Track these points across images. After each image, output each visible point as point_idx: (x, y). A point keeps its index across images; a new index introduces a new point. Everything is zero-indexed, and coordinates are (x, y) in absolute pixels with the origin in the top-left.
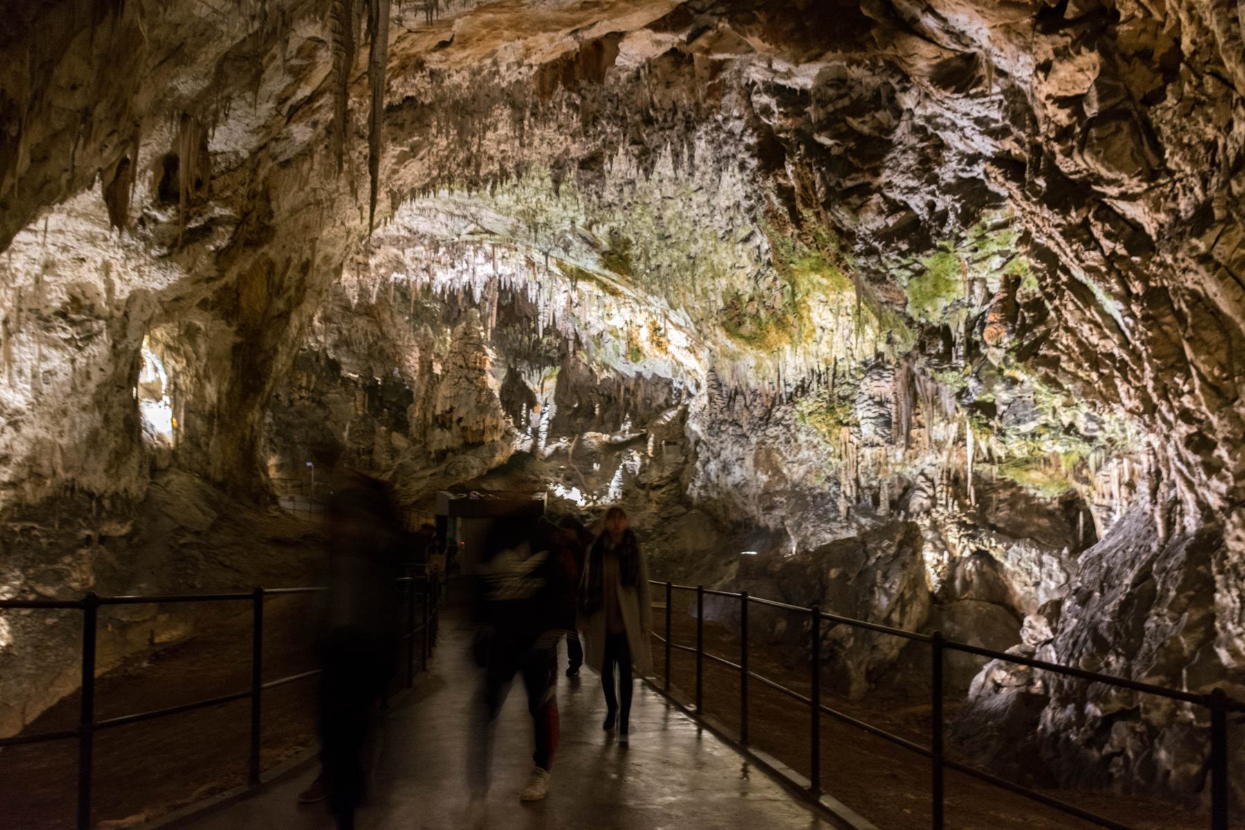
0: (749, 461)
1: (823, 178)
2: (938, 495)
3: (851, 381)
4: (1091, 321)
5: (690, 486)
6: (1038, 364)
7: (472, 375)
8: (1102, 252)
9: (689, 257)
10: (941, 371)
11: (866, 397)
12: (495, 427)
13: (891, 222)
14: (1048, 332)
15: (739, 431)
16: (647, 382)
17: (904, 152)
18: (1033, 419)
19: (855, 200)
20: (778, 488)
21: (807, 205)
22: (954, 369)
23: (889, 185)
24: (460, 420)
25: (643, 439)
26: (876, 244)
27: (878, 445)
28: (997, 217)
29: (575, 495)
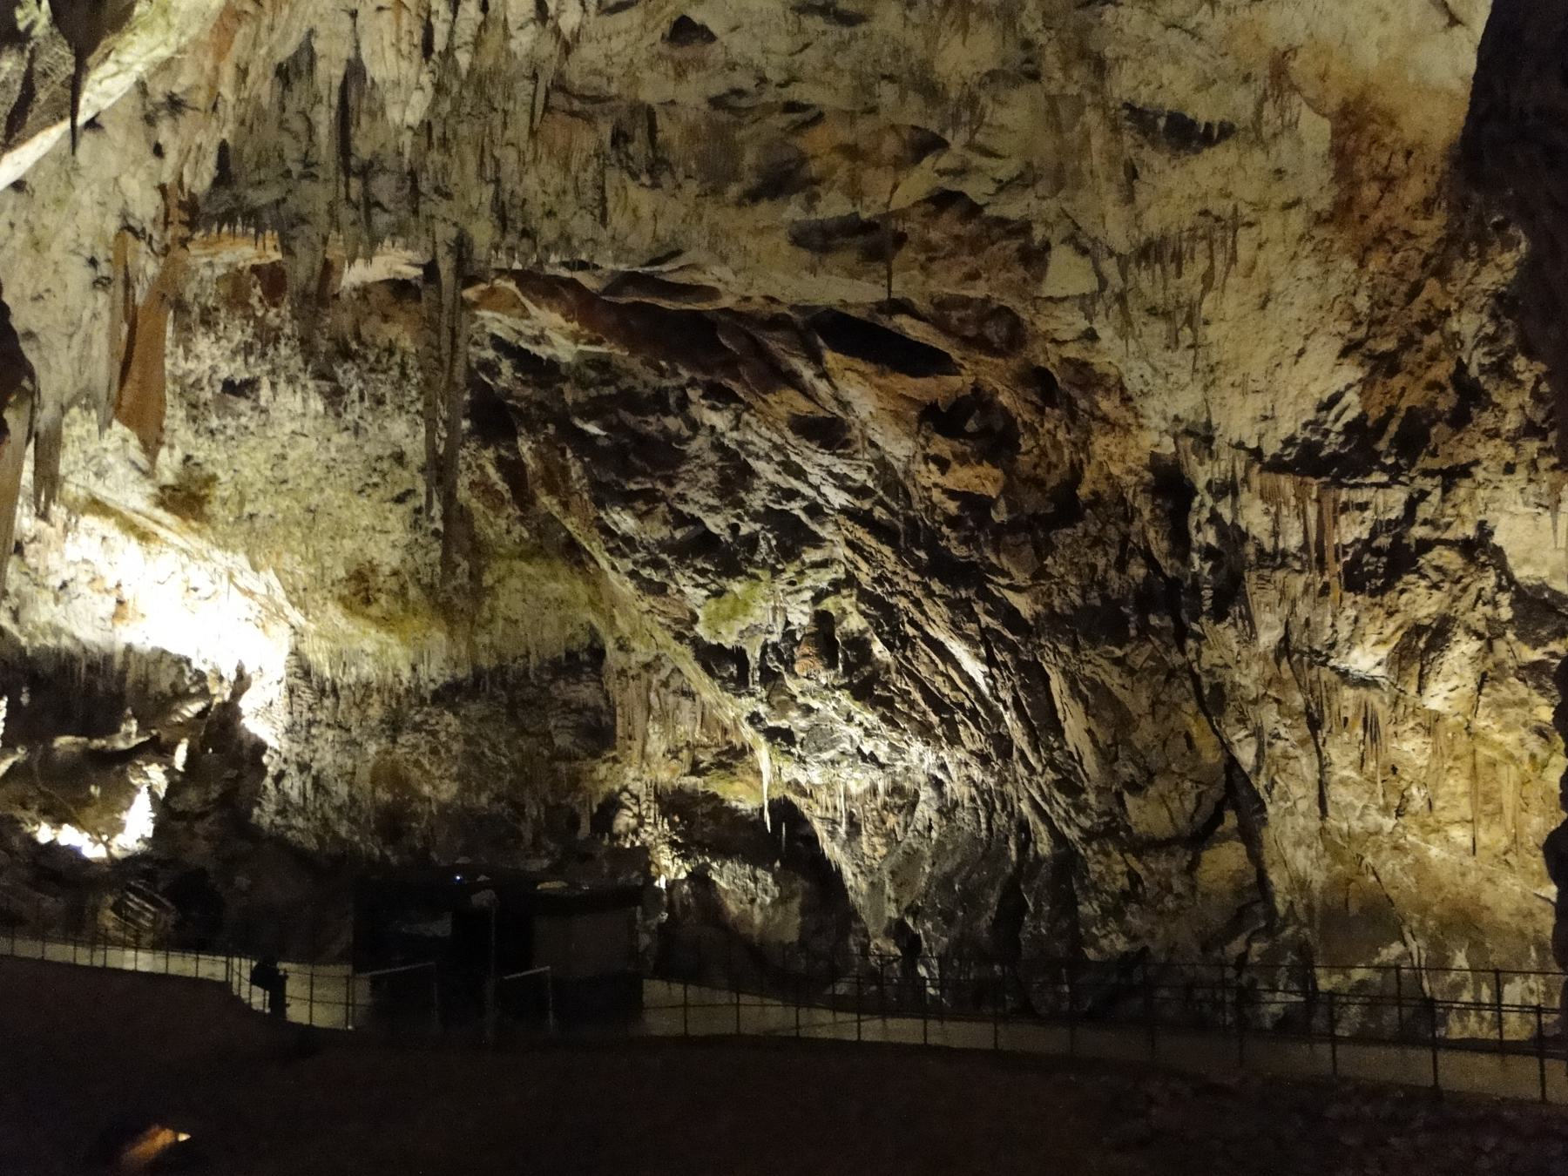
5: (256, 811)
9: (309, 510)
10: (740, 696)
13: (678, 535)
15: (345, 736)
17: (703, 468)
19: (641, 506)
21: (552, 490)
22: (752, 695)
23: (682, 498)
26: (664, 556)
29: (69, 836)
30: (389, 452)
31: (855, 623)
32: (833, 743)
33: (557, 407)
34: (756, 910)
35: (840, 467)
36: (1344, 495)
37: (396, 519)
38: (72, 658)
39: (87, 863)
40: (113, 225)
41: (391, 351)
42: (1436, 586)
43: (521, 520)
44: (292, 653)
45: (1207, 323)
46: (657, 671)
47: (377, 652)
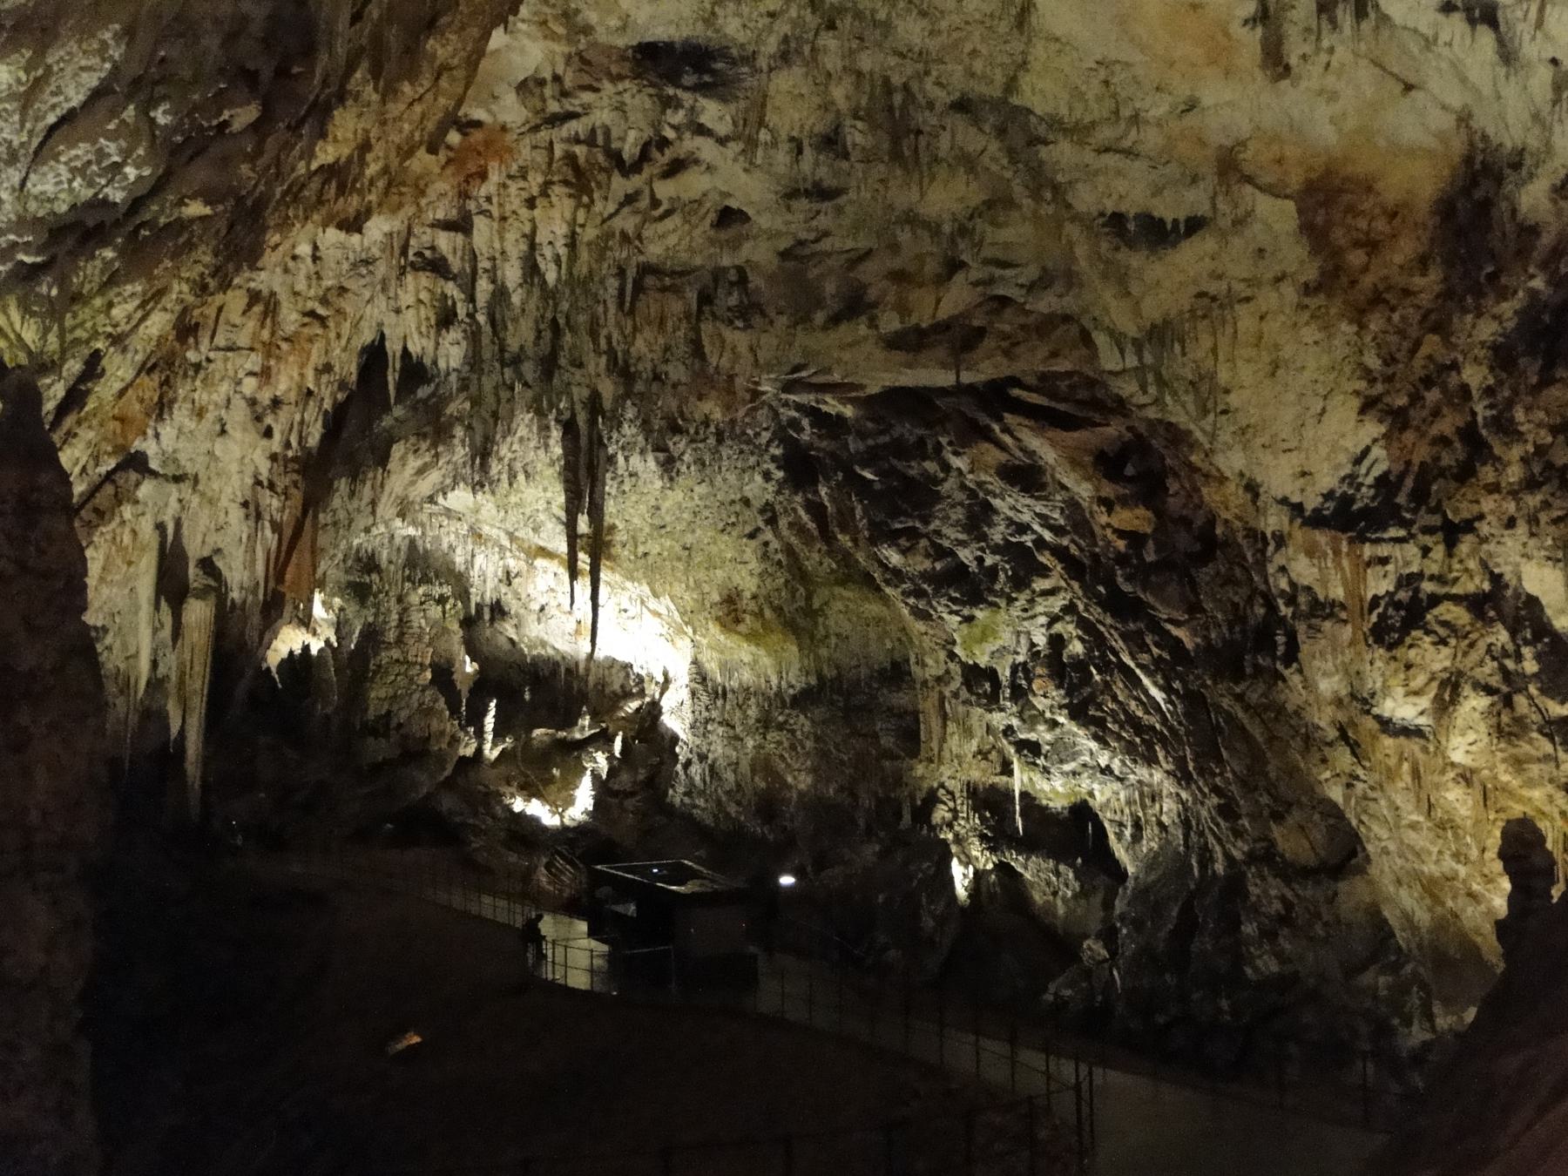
1: (865, 510)
4: (1137, 699)
5: (671, 792)
9: (685, 548)
10: (990, 711)
12: (442, 733)
13: (938, 566)
15: (731, 733)
17: (953, 506)
19: (903, 542)
21: (844, 530)
22: (1002, 710)
23: (938, 533)
25: (603, 739)
29: (536, 809)
31: (1077, 648)
32: (1074, 756)
33: (845, 455)
34: (1059, 903)
35: (1039, 508)
36: (1368, 551)
37: (750, 550)
38: (556, 664)
39: (545, 829)
40: (250, 481)
41: (706, 422)
42: (1443, 642)
45: (1227, 391)
46: (947, 684)
47: (755, 663)
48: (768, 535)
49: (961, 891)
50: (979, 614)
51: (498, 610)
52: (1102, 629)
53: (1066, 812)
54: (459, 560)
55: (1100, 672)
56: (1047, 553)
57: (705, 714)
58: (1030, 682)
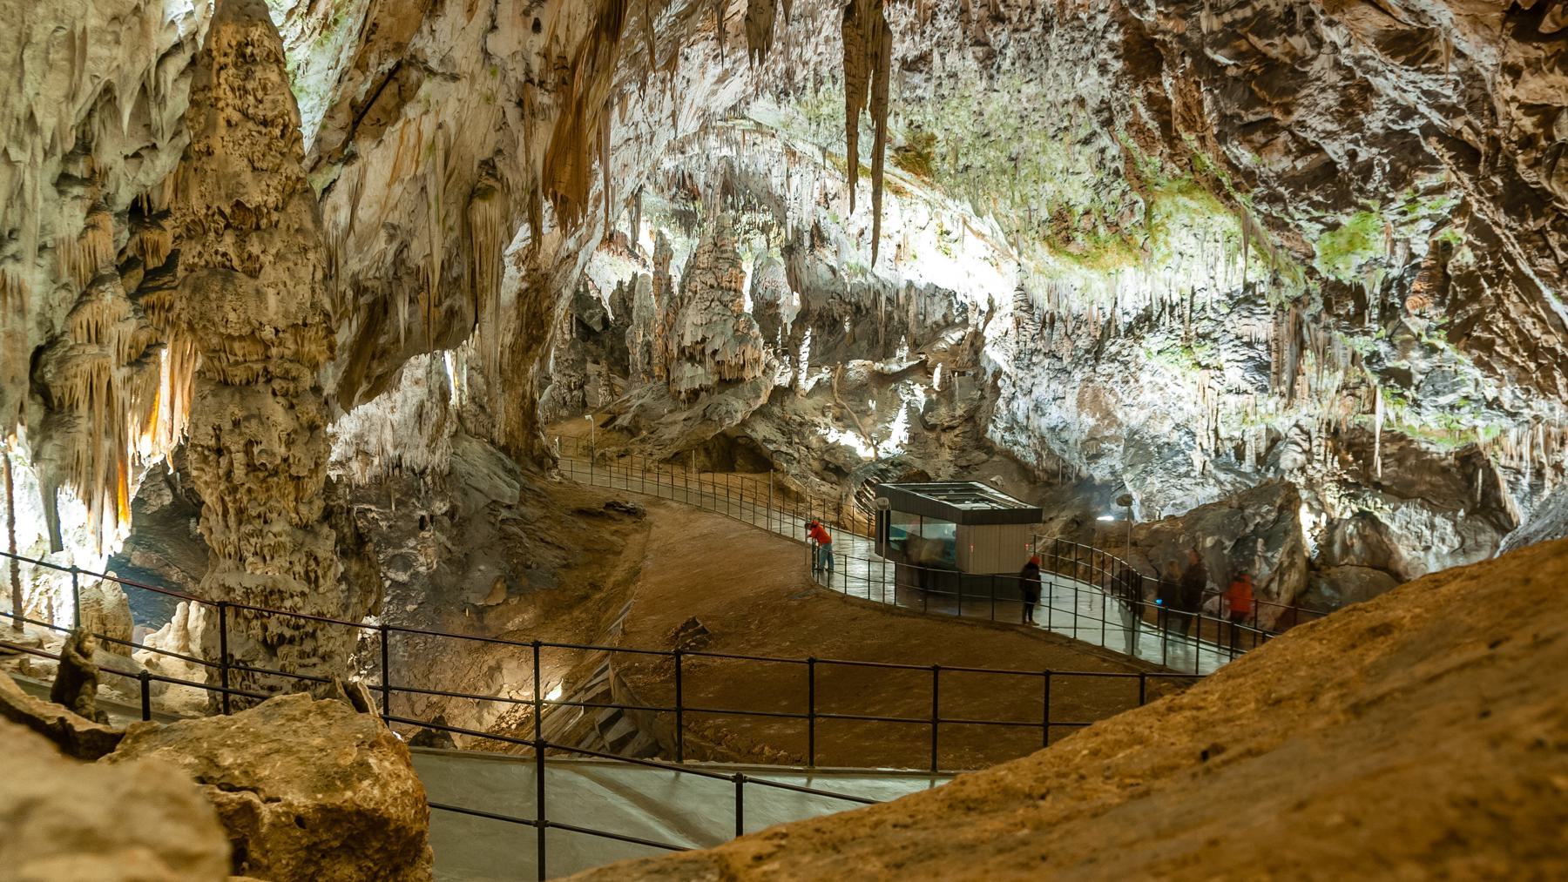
0: (1071, 400)
1: (1216, 102)
2: (1315, 450)
3: (1213, 316)
4: (1534, 315)
5: (991, 427)
6: (1472, 347)
7: (727, 298)
8: (1556, 260)
9: (1011, 159)
10: (1352, 335)
11: (1232, 337)
12: (757, 361)
13: (1300, 165)
14: (1482, 313)
15: (1058, 365)
16: (920, 293)
17: (1323, 90)
18: (1454, 391)
20: (1107, 433)
21: (1190, 127)
24: (715, 352)
25: (924, 369)
26: (1282, 189)
27: (1246, 392)
28: (1433, 180)
29: (849, 439)
30: (1072, 96)
33: (1195, 37)
39: (859, 461)
43: (1171, 157)
44: (1019, 289)
46: (1306, 306)
48: (1104, 141)
49: (1310, 544)
50: (1344, 220)
51: (818, 236)
52: (1498, 231)
53: (1451, 459)
54: (776, 181)
55: (1491, 285)
56: (1433, 140)
57: (1031, 345)
58: (1403, 299)
